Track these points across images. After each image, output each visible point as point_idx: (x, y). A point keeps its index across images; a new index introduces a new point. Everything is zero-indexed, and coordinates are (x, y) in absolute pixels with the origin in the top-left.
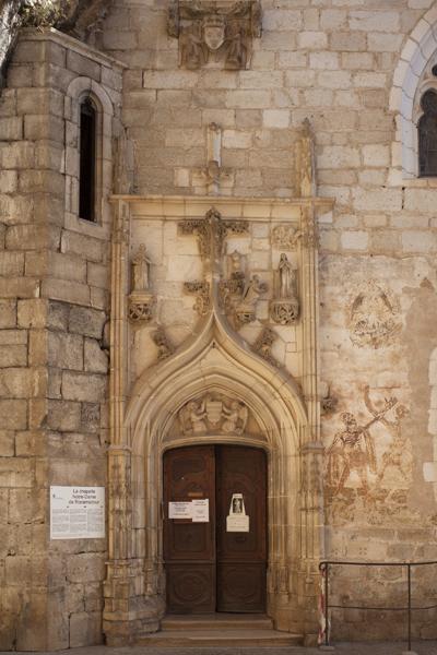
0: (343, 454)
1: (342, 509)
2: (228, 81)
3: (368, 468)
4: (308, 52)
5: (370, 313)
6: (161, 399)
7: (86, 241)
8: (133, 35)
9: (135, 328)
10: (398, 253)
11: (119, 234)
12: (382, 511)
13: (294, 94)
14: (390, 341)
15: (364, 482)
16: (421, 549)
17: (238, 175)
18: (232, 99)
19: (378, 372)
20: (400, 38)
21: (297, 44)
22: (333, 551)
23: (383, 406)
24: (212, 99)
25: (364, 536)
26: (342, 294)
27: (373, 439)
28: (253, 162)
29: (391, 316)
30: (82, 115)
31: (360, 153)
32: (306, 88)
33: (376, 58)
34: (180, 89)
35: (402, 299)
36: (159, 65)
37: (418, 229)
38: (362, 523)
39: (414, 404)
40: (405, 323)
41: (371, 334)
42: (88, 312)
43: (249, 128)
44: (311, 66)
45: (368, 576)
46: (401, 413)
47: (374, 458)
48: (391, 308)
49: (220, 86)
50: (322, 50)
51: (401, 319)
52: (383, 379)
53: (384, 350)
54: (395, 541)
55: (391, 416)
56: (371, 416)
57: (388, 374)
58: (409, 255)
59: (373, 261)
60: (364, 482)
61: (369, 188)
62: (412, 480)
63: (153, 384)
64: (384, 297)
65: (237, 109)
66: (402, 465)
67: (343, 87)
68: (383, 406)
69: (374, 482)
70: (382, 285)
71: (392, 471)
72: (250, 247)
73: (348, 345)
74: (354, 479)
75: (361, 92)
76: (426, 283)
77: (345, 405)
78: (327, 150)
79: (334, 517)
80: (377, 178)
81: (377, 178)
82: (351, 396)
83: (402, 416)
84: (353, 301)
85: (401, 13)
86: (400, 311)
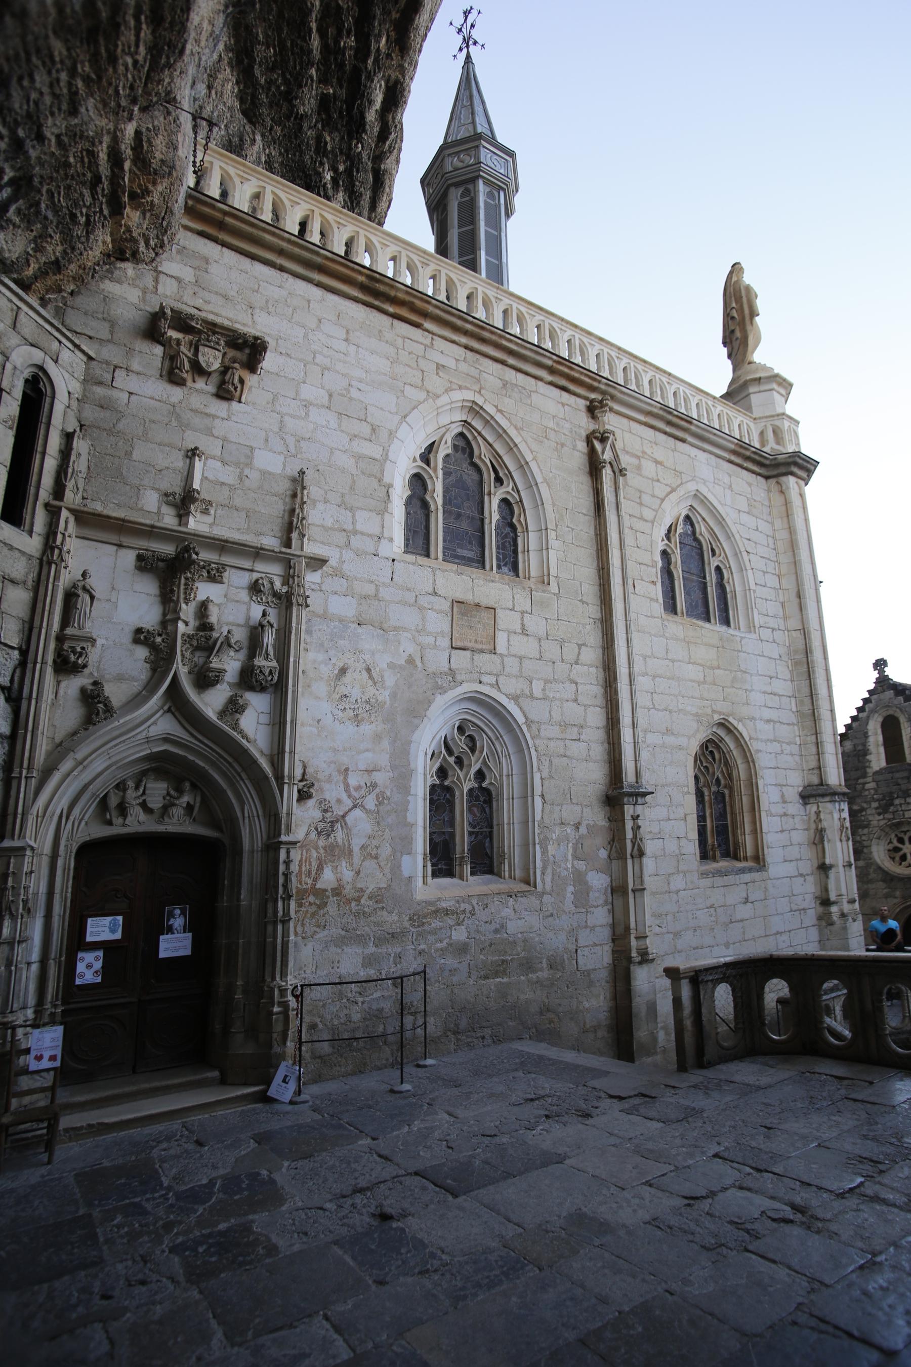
0: (316, 848)
1: (314, 915)
2: (219, 408)
3: (344, 863)
4: (307, 405)
5: (355, 685)
6: (86, 776)
7: (5, 550)
8: (107, 325)
9: (60, 678)
10: (385, 626)
11: (56, 551)
12: (357, 915)
13: (291, 441)
15: (339, 880)
16: (399, 956)
17: (219, 512)
18: (220, 428)
20: (397, 418)
21: (297, 393)
22: (300, 969)
23: (363, 792)
24: (197, 421)
25: (336, 946)
28: (238, 502)
29: (375, 691)
30: (25, 394)
31: (354, 516)
32: (303, 439)
33: (374, 430)
34: (159, 401)
35: (386, 675)
36: (135, 366)
37: (405, 604)
38: (335, 931)
39: (394, 789)
40: (388, 702)
41: (354, 710)
43: (237, 464)
44: (310, 419)
45: (341, 995)
46: (381, 800)
47: (351, 851)
48: (375, 683)
49: (208, 411)
50: (323, 406)
51: (384, 696)
52: (364, 760)
53: (367, 729)
54: (371, 949)
55: (370, 802)
56: (349, 803)
57: (369, 755)
58: (396, 629)
59: (360, 630)
60: (339, 880)
61: (359, 553)
63: (79, 756)
64: (368, 670)
65: (225, 439)
66: (381, 859)
67: (341, 447)
68: (363, 792)
69: (350, 880)
71: (370, 864)
72: (225, 596)
73: (328, 720)
74: (328, 878)
75: (358, 457)
76: (410, 661)
77: (321, 790)
78: (320, 506)
79: (303, 925)
80: (370, 546)
81: (370, 546)
82: (329, 780)
83: (380, 803)
84: (336, 672)
85: (398, 398)
86: (385, 688)
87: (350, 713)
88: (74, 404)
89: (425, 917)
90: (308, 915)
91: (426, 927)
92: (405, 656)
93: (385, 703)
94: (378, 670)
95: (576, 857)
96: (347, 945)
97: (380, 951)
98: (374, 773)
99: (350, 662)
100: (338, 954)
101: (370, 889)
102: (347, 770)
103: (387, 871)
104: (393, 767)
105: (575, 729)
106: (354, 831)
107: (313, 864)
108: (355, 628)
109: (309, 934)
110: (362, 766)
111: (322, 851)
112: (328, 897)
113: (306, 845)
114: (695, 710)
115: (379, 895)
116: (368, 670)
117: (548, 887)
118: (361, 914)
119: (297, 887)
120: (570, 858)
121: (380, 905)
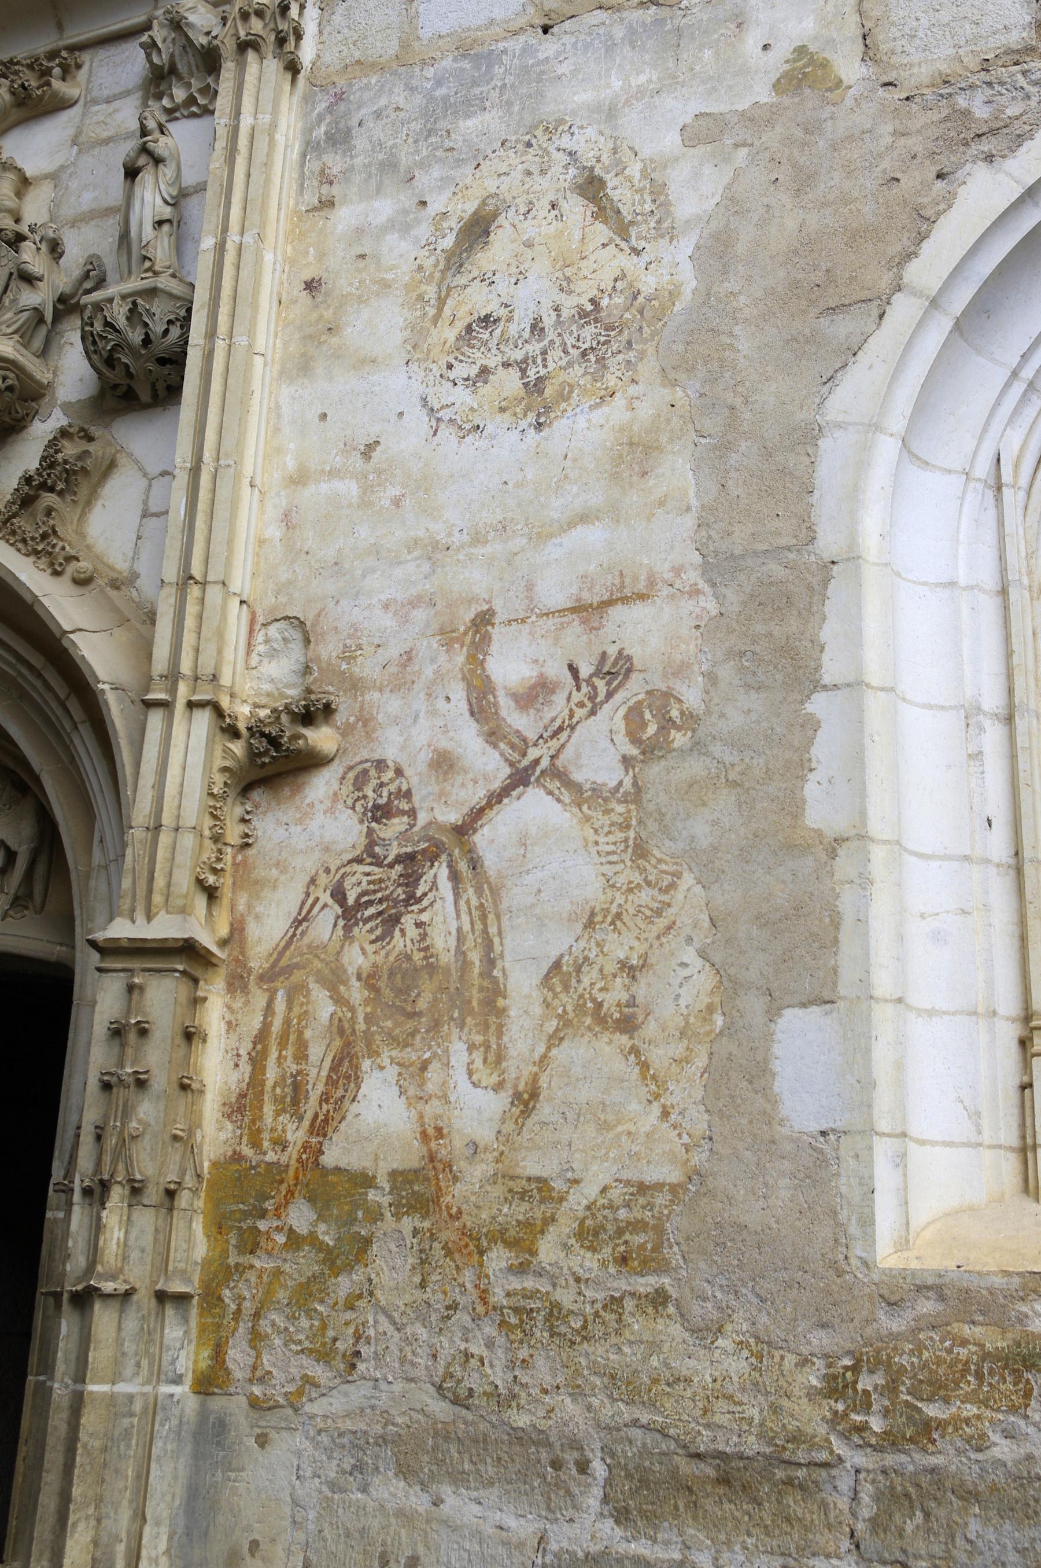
3: (459, 1052)
12: (520, 1319)
14: (611, 380)
15: (432, 1134)
19: (541, 536)
23: (558, 707)
25: (405, 1471)
26: (402, 225)
27: (495, 892)
29: (626, 261)
35: (677, 178)
38: (395, 1389)
39: (726, 673)
41: (523, 366)
47: (493, 998)
48: (623, 230)
51: (672, 266)
53: (585, 428)
55: (598, 752)
56: (490, 765)
59: (549, 47)
60: (432, 1134)
62: (698, 1121)
64: (591, 187)
66: (650, 1029)
68: (558, 707)
69: (485, 1135)
70: (588, 143)
71: (591, 1062)
73: (408, 440)
77: (366, 720)
79: (256, 1338)
82: (402, 674)
83: (651, 750)
84: (448, 242)
87: (510, 382)
89: (938, 1389)
90: (282, 1295)
91: (946, 1456)
92: (777, 62)
93: (674, 295)
94: (634, 170)
96: (459, 1479)
97: (639, 1548)
98: (617, 613)
99: (509, 186)
100: (404, 1515)
101: (590, 1191)
102: (484, 620)
103: (686, 1092)
104: (719, 566)
106: (515, 896)
107: (315, 1052)
108: (528, 50)
109: (279, 1389)
110: (555, 592)
111: (356, 993)
112: (375, 1216)
113: (289, 970)
115: (637, 1226)
116: (591, 187)
118: (530, 1320)
119: (237, 1157)
121: (646, 1284)
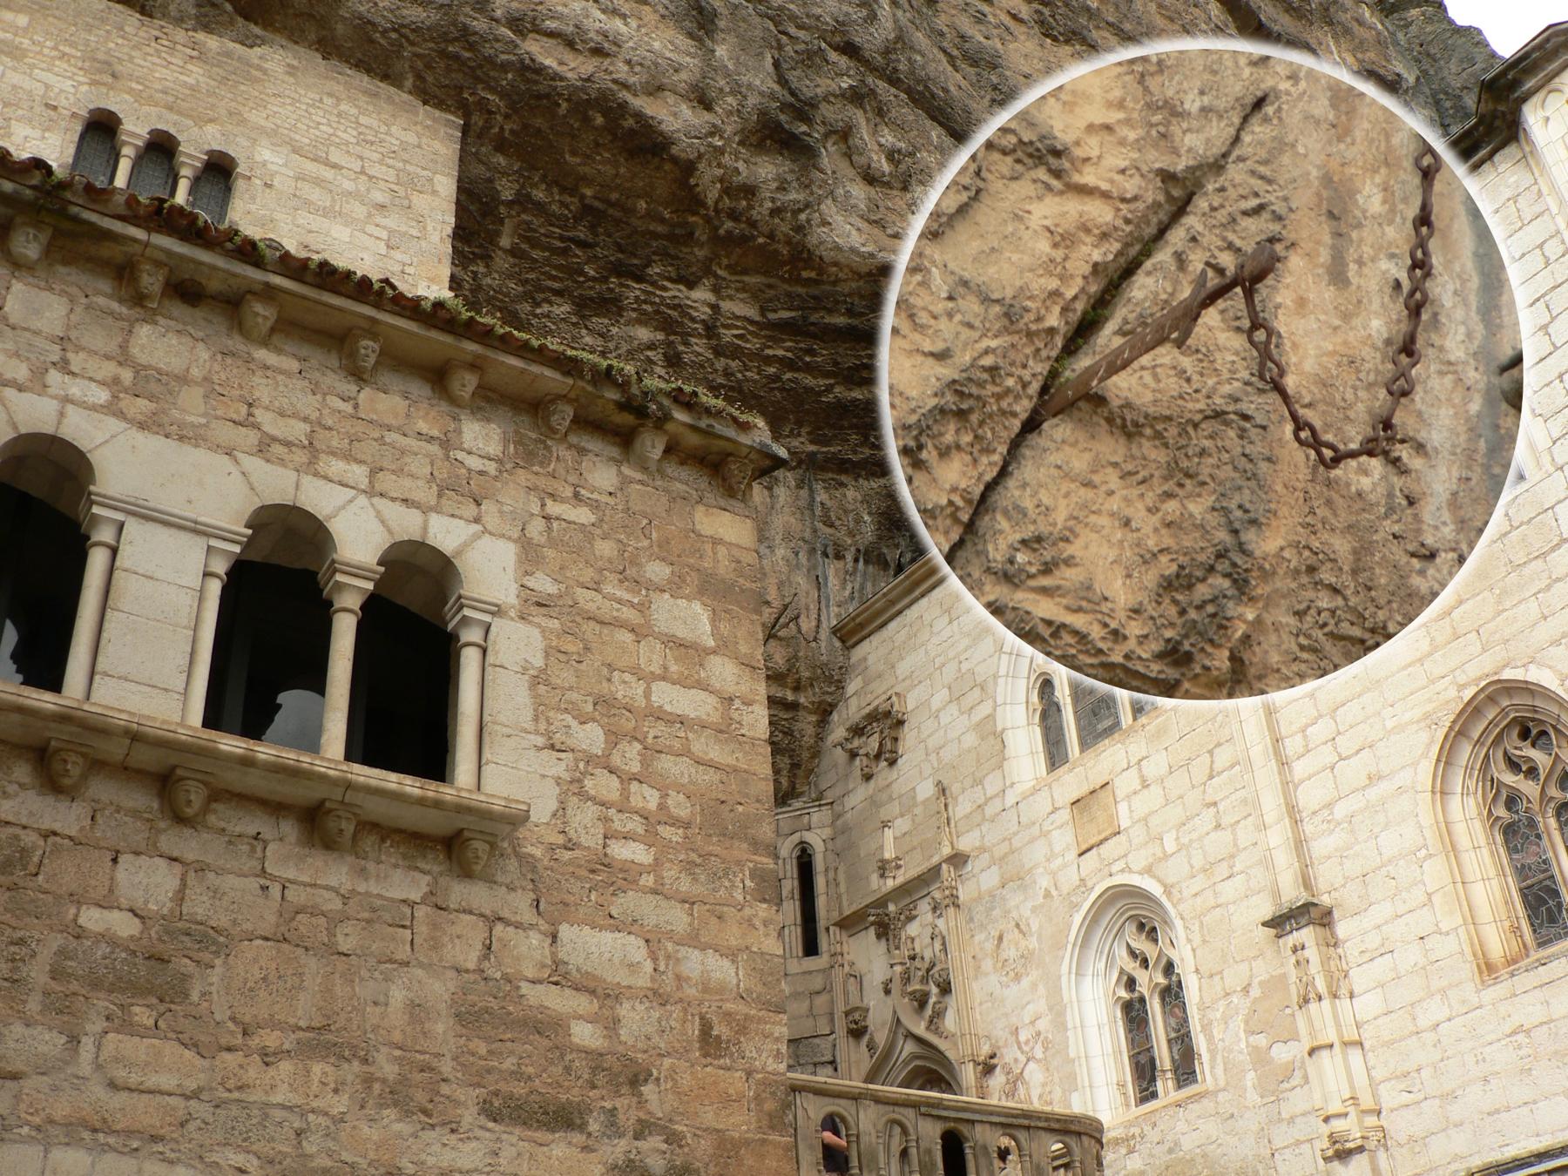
2: (894, 774)
26: (987, 939)
42: (817, 1041)
56: (1023, 1059)
88: (830, 845)
95: (1250, 1032)
104: (1051, 1009)
105: (1225, 865)
114: (1417, 713)
116: (1018, 926)
117: (1222, 1083)
120: (1242, 1035)
